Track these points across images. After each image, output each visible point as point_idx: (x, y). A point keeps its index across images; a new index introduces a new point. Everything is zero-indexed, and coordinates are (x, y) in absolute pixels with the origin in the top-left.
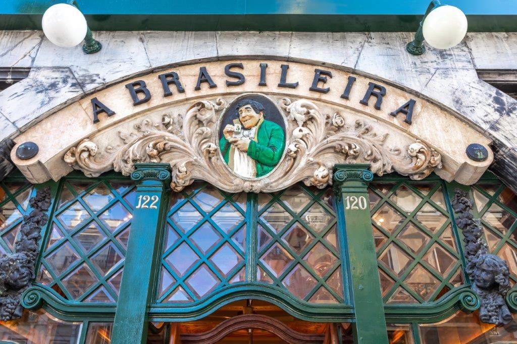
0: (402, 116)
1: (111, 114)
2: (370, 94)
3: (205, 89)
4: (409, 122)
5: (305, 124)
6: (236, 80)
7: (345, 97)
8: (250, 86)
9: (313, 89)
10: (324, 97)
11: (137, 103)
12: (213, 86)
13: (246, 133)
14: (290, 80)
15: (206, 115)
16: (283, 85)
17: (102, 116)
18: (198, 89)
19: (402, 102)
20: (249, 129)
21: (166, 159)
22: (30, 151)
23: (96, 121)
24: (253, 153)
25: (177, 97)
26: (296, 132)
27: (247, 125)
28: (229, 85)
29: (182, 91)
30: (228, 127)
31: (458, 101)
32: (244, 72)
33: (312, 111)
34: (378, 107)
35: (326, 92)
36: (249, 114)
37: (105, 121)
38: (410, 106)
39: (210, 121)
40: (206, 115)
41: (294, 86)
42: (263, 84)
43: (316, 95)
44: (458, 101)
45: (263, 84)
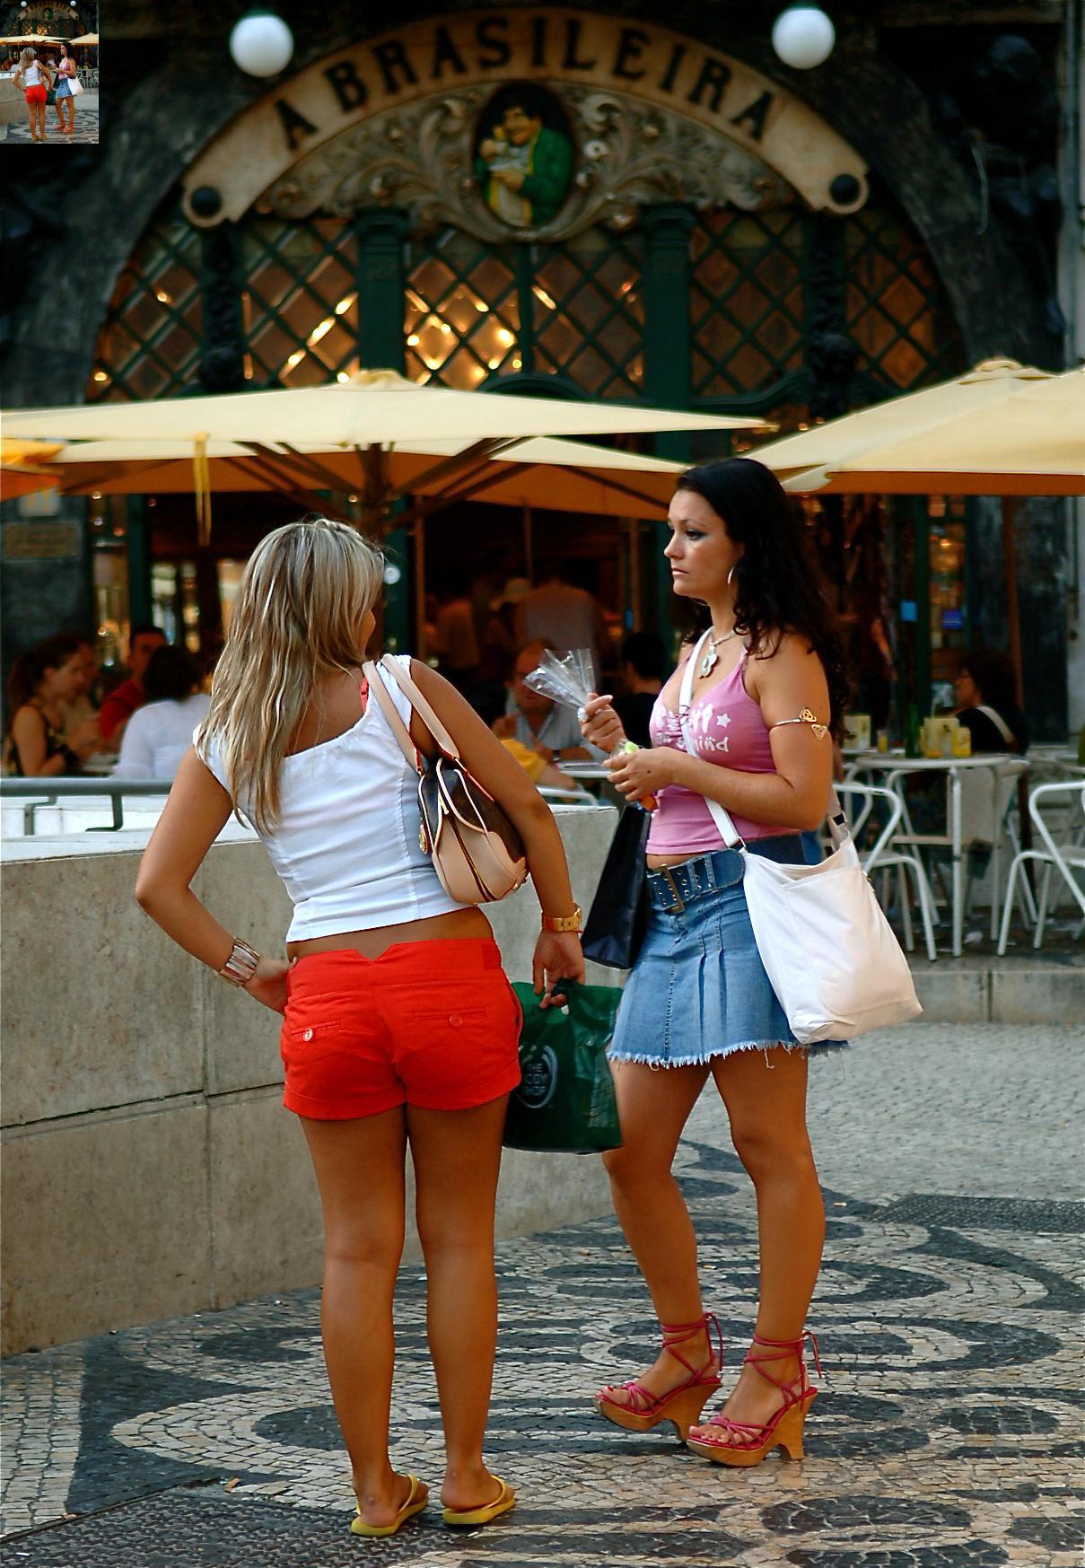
0: (749, 124)
1: (310, 129)
2: (705, 77)
3: (450, 77)
4: (757, 134)
5: (603, 136)
6: (493, 55)
7: (667, 85)
8: (518, 69)
9: (619, 71)
10: (638, 87)
11: (347, 106)
13: (515, 151)
15: (453, 125)
17: (298, 132)
18: (437, 73)
19: (754, 95)
20: (521, 145)
21: (402, 199)
23: (293, 144)
24: (523, 192)
25: (408, 91)
26: (591, 149)
27: (519, 137)
28: (486, 64)
30: (489, 146)
33: (616, 116)
34: (715, 106)
35: (636, 76)
36: (518, 120)
37: (309, 143)
39: (458, 134)
40: (453, 125)
42: (538, 60)
43: (622, 83)
45: (538, 60)
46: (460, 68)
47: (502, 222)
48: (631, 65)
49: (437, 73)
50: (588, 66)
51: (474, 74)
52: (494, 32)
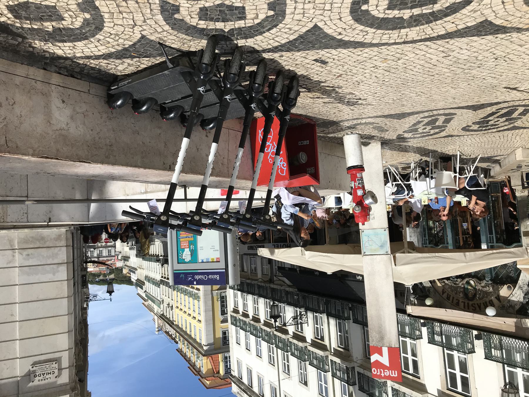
1: (496, 298)
2: (449, 298)
6: (474, 305)
9: (459, 301)
12: (478, 304)
14: (463, 304)
16: (464, 303)
22: (509, 287)
29: (483, 303)
31: (435, 293)
32: (472, 308)
35: (457, 300)
38: (443, 294)
41: (462, 302)
42: (468, 304)
44: (435, 293)
46: (478, 304)
47: (473, 281)
48: (457, 301)
49: (480, 304)
50: (462, 302)
51: (476, 303)
52: (474, 309)
